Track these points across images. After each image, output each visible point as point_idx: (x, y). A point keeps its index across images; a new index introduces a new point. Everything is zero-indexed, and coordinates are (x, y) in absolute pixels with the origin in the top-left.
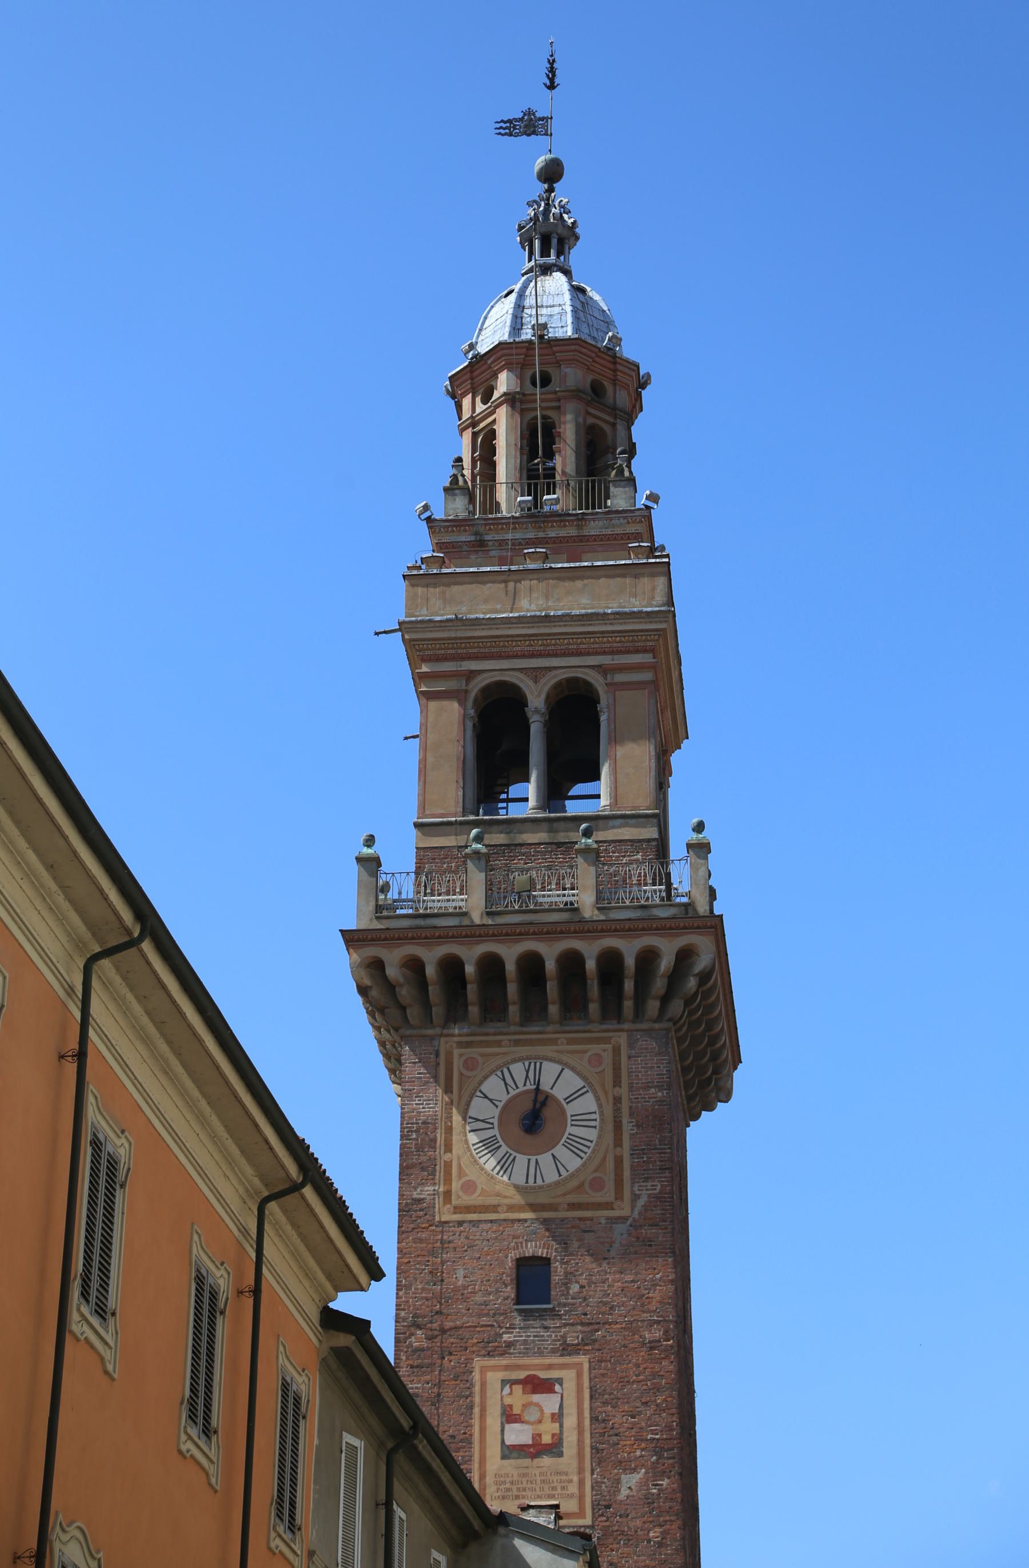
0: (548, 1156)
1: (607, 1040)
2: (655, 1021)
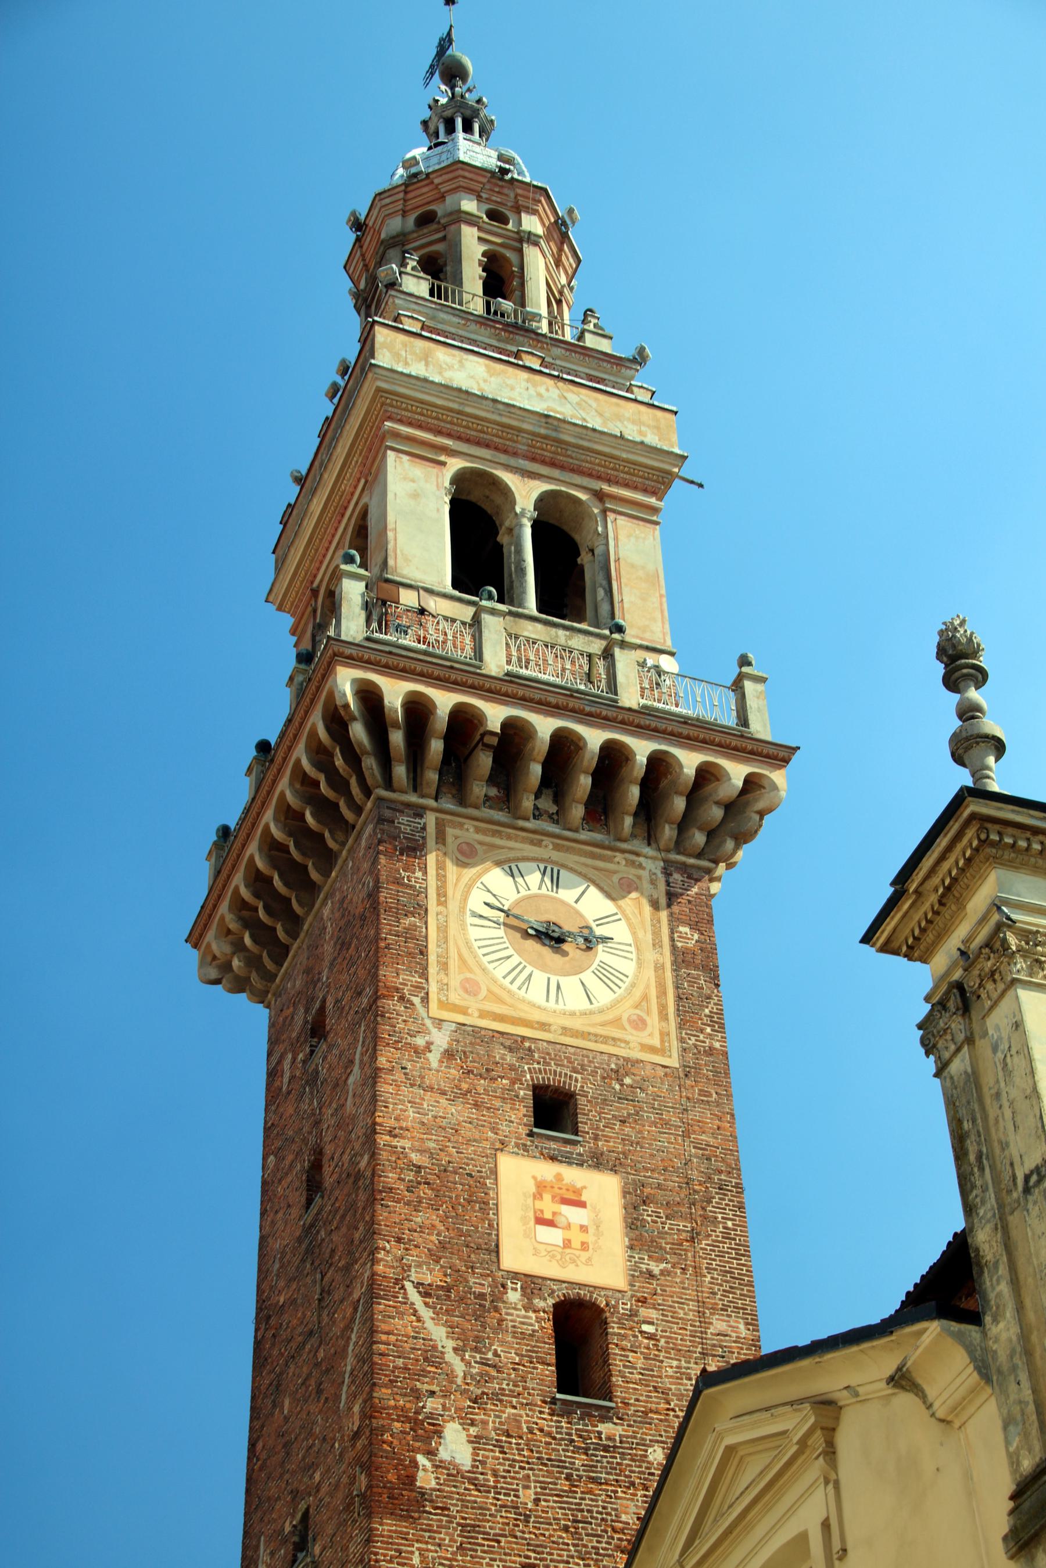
0: (574, 980)
1: (640, 866)
2: (699, 856)
